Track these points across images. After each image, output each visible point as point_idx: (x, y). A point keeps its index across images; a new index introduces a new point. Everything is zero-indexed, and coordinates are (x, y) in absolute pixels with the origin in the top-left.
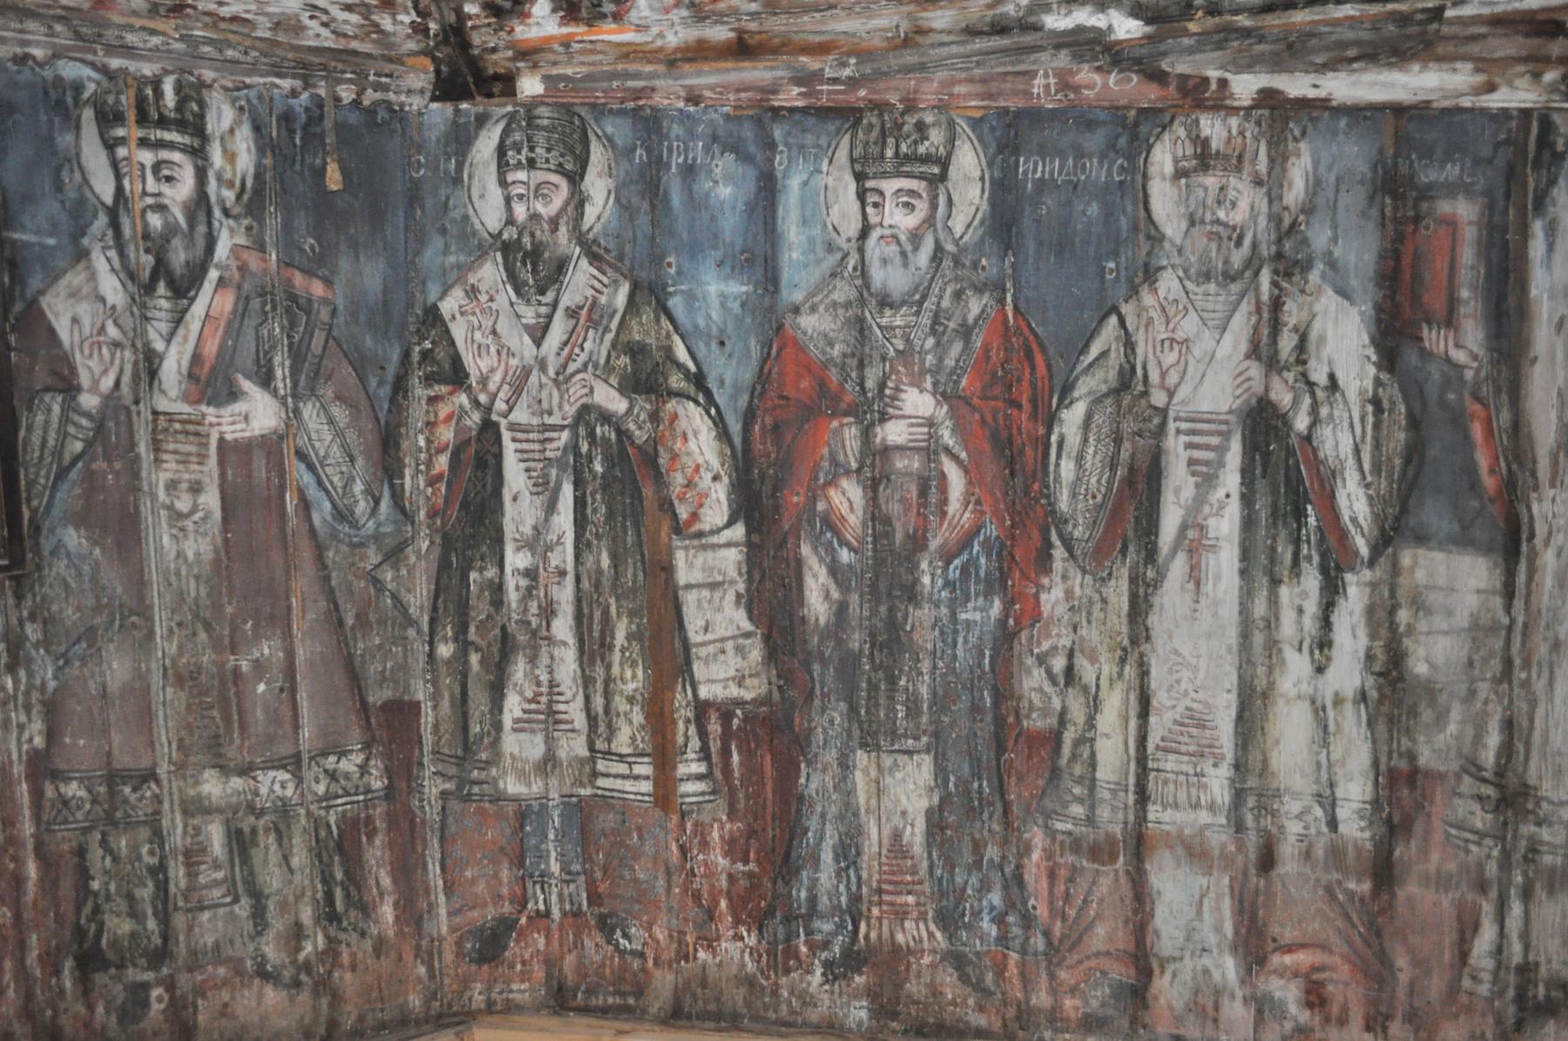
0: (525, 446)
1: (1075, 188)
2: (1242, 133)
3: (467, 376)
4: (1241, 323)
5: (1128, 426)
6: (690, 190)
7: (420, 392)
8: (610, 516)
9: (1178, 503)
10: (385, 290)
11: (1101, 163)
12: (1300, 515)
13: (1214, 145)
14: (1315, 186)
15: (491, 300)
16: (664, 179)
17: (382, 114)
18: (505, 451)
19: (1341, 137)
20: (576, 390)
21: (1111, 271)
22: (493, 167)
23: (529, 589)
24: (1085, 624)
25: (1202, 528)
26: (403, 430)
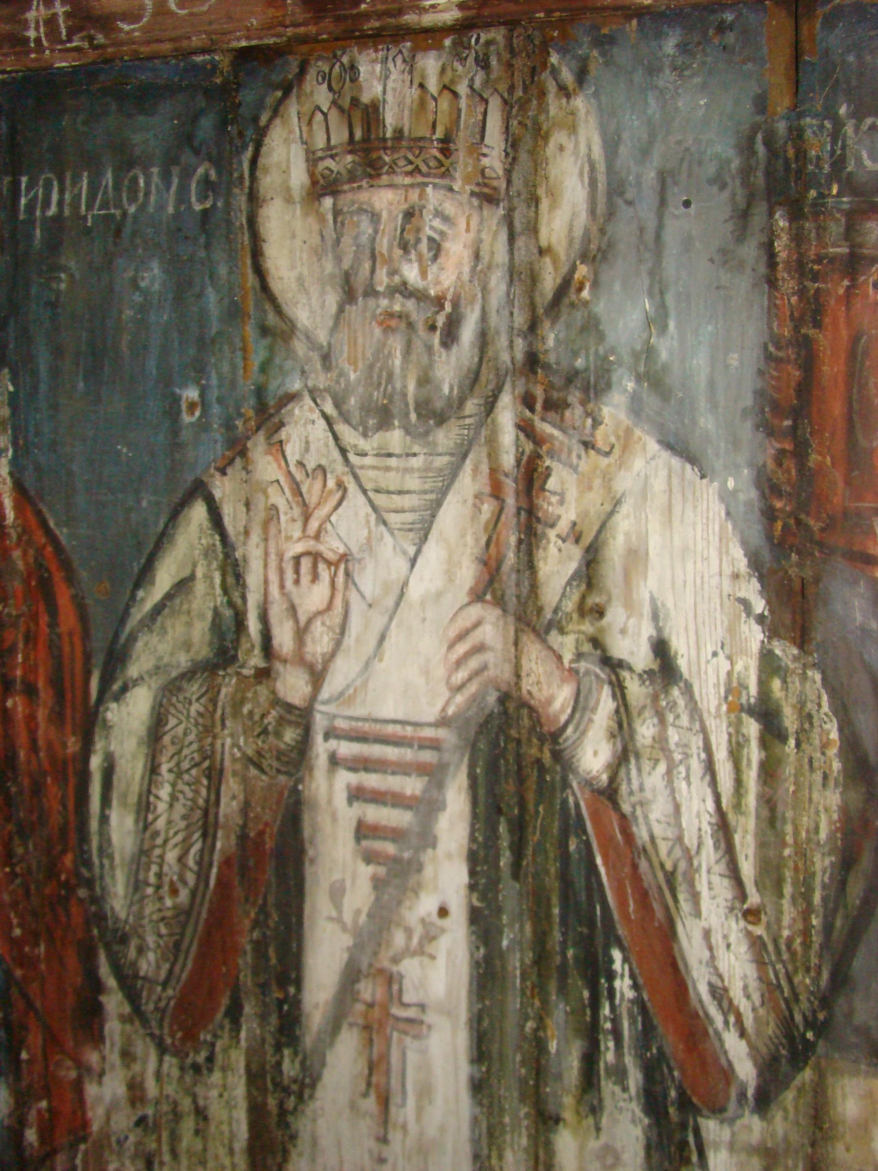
1: (118, 233)
2: (447, 88)
4: (460, 521)
5: (233, 744)
9: (339, 920)
11: (166, 176)
12: (596, 971)
13: (390, 119)
14: (611, 194)
19: (667, 78)
21: (192, 406)
24: (167, 1157)
25: (390, 980)
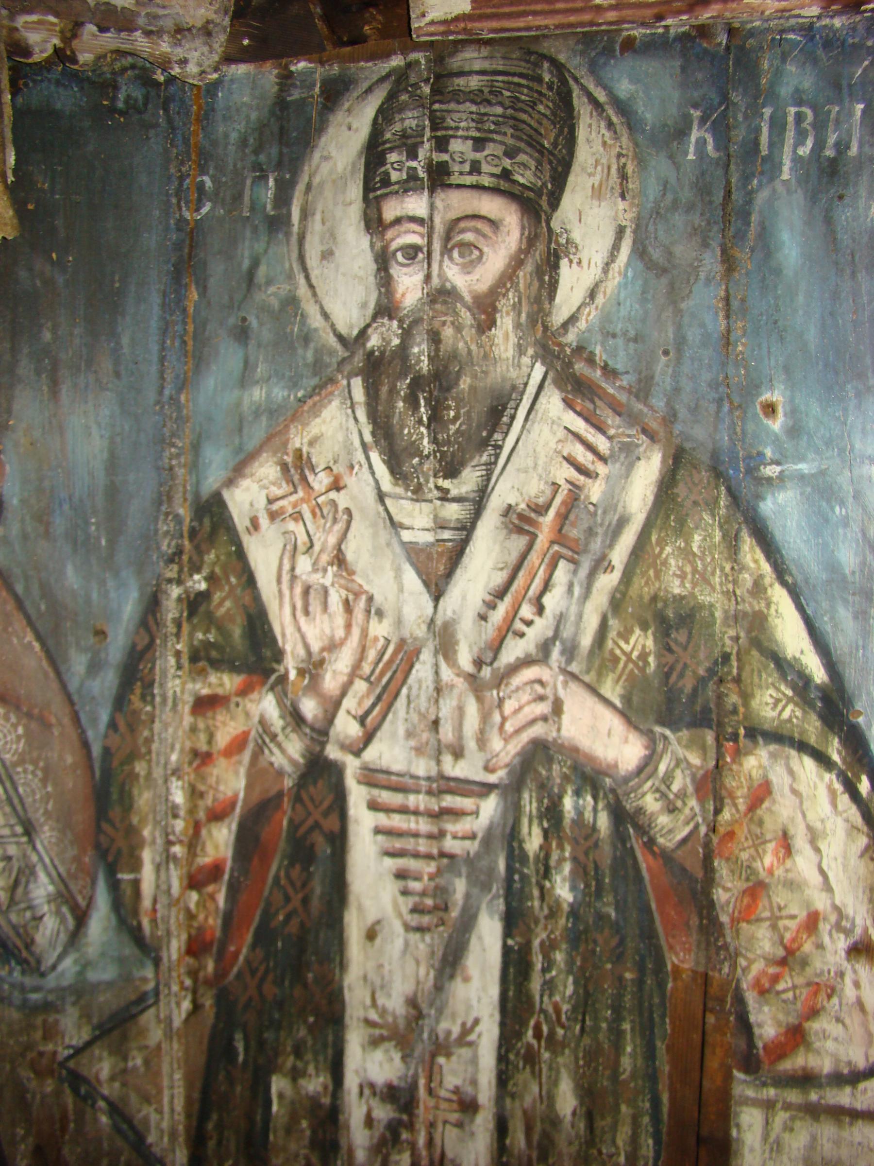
0: (397, 821)
3: (278, 655)
6: (828, 221)
7: (177, 685)
8: (584, 1003)
10: (112, 464)
15: (337, 486)
16: (762, 197)
17: (128, 91)
18: (352, 828)
20: (520, 705)
22: (355, 191)
23: (394, 1129)
26: (140, 767)
